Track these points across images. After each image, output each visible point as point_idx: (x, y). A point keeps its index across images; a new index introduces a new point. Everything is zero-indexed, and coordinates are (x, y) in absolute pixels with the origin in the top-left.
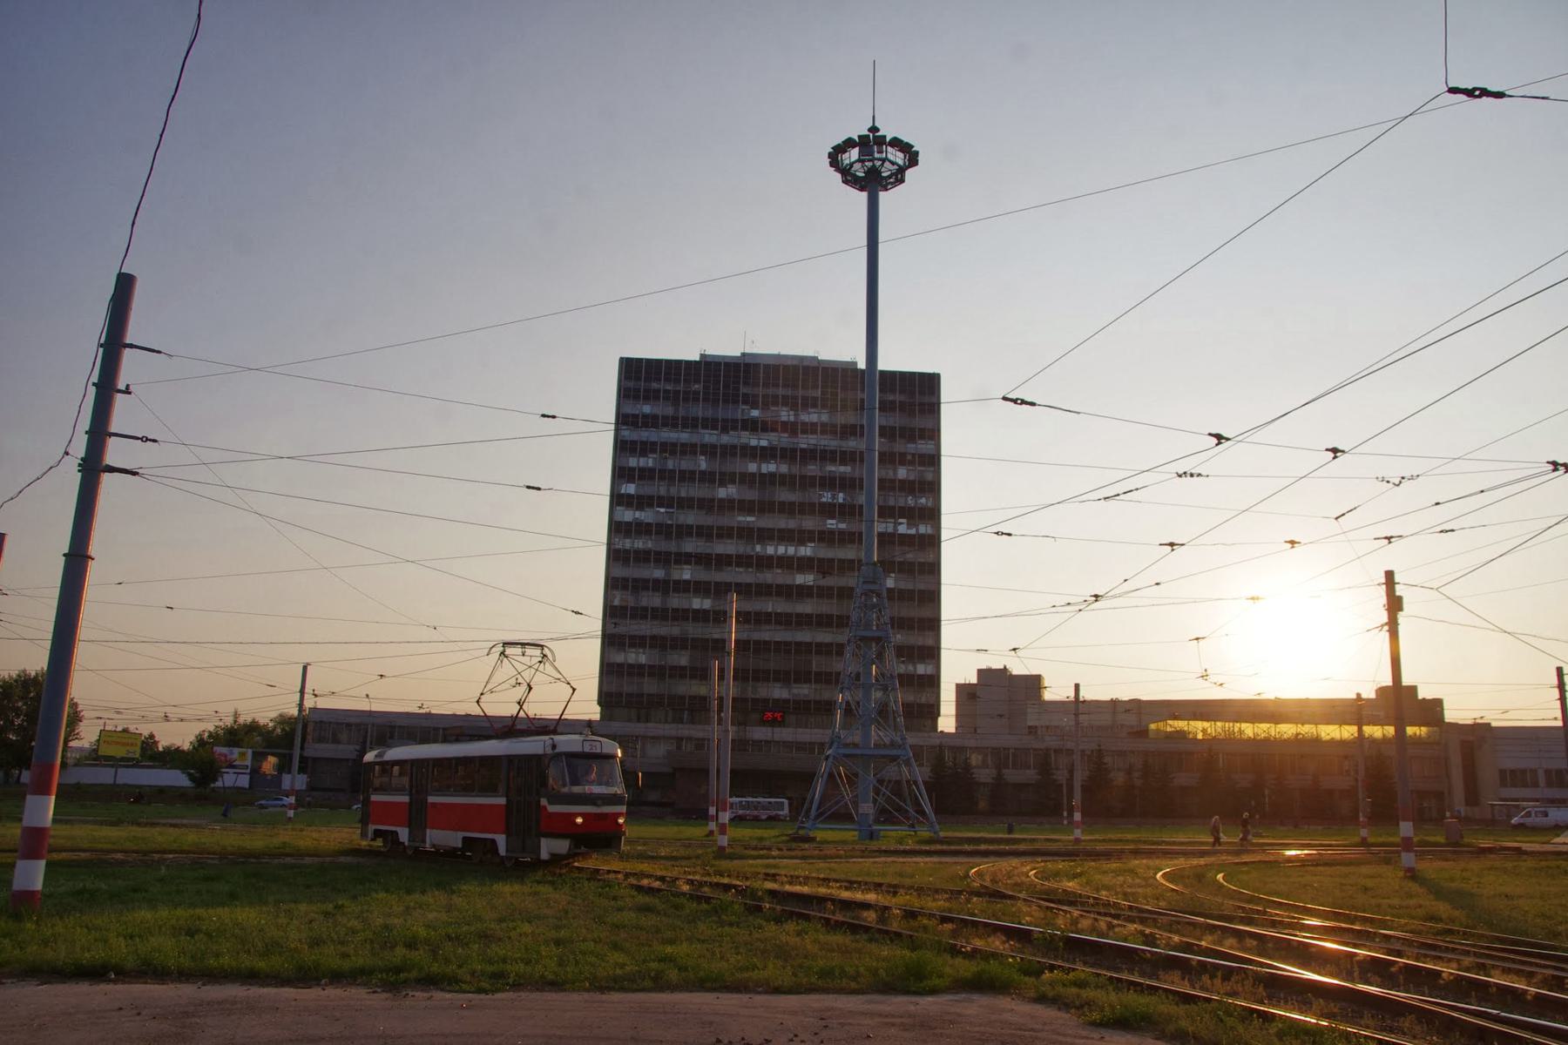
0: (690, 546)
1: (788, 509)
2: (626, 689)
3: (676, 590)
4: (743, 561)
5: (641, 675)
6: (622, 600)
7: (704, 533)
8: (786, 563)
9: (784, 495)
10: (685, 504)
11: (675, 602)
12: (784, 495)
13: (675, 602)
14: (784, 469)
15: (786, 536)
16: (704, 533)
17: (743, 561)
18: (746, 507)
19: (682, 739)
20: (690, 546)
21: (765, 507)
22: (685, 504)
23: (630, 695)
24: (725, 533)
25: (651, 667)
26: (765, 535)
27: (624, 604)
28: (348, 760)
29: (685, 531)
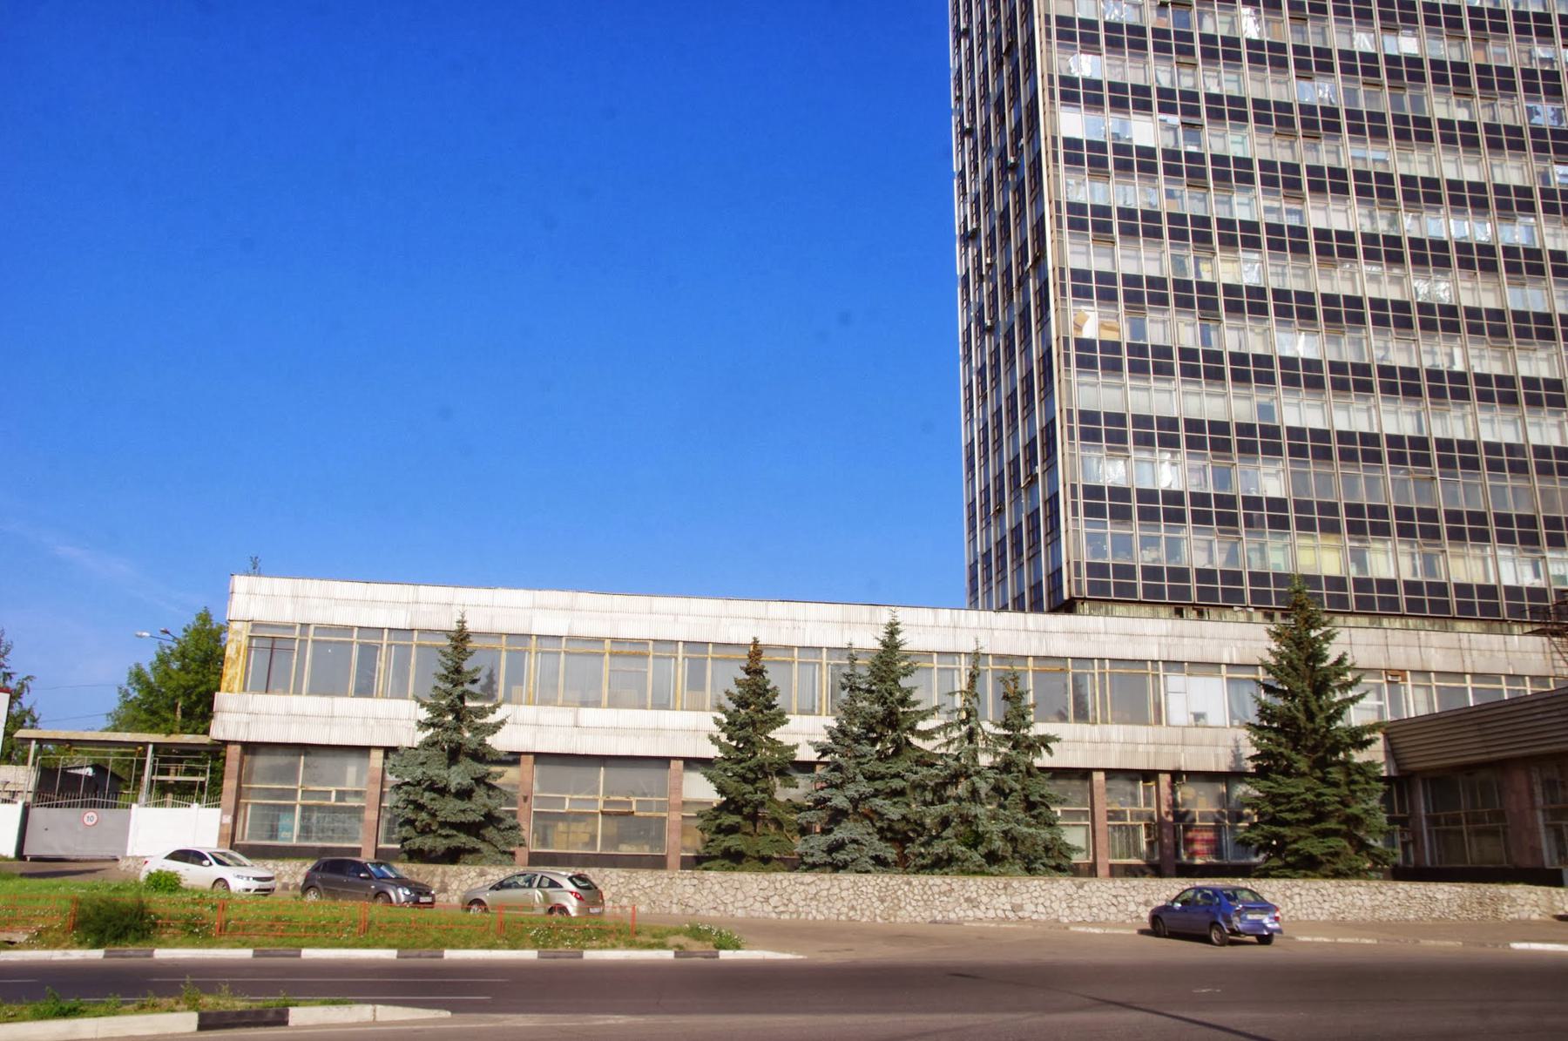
0: (1250, 205)
1: (1462, 136)
2: (1143, 558)
3: (1234, 308)
4: (1387, 250)
5: (1176, 517)
6: (1102, 326)
7: (1282, 179)
8: (1479, 259)
9: (1441, 107)
10: (1229, 110)
11: (1235, 337)
12: (1441, 107)
13: (1235, 337)
14: (1445, 50)
15: (1468, 197)
16: (1282, 179)
17: (1387, 250)
18: (1369, 126)
19: (1401, 673)
20: (1250, 205)
21: (1416, 131)
22: (1229, 110)
23: (1152, 572)
24: (1331, 182)
25: (1200, 499)
26: (1425, 192)
27: (1111, 336)
28: (364, 750)
29: (1234, 173)
